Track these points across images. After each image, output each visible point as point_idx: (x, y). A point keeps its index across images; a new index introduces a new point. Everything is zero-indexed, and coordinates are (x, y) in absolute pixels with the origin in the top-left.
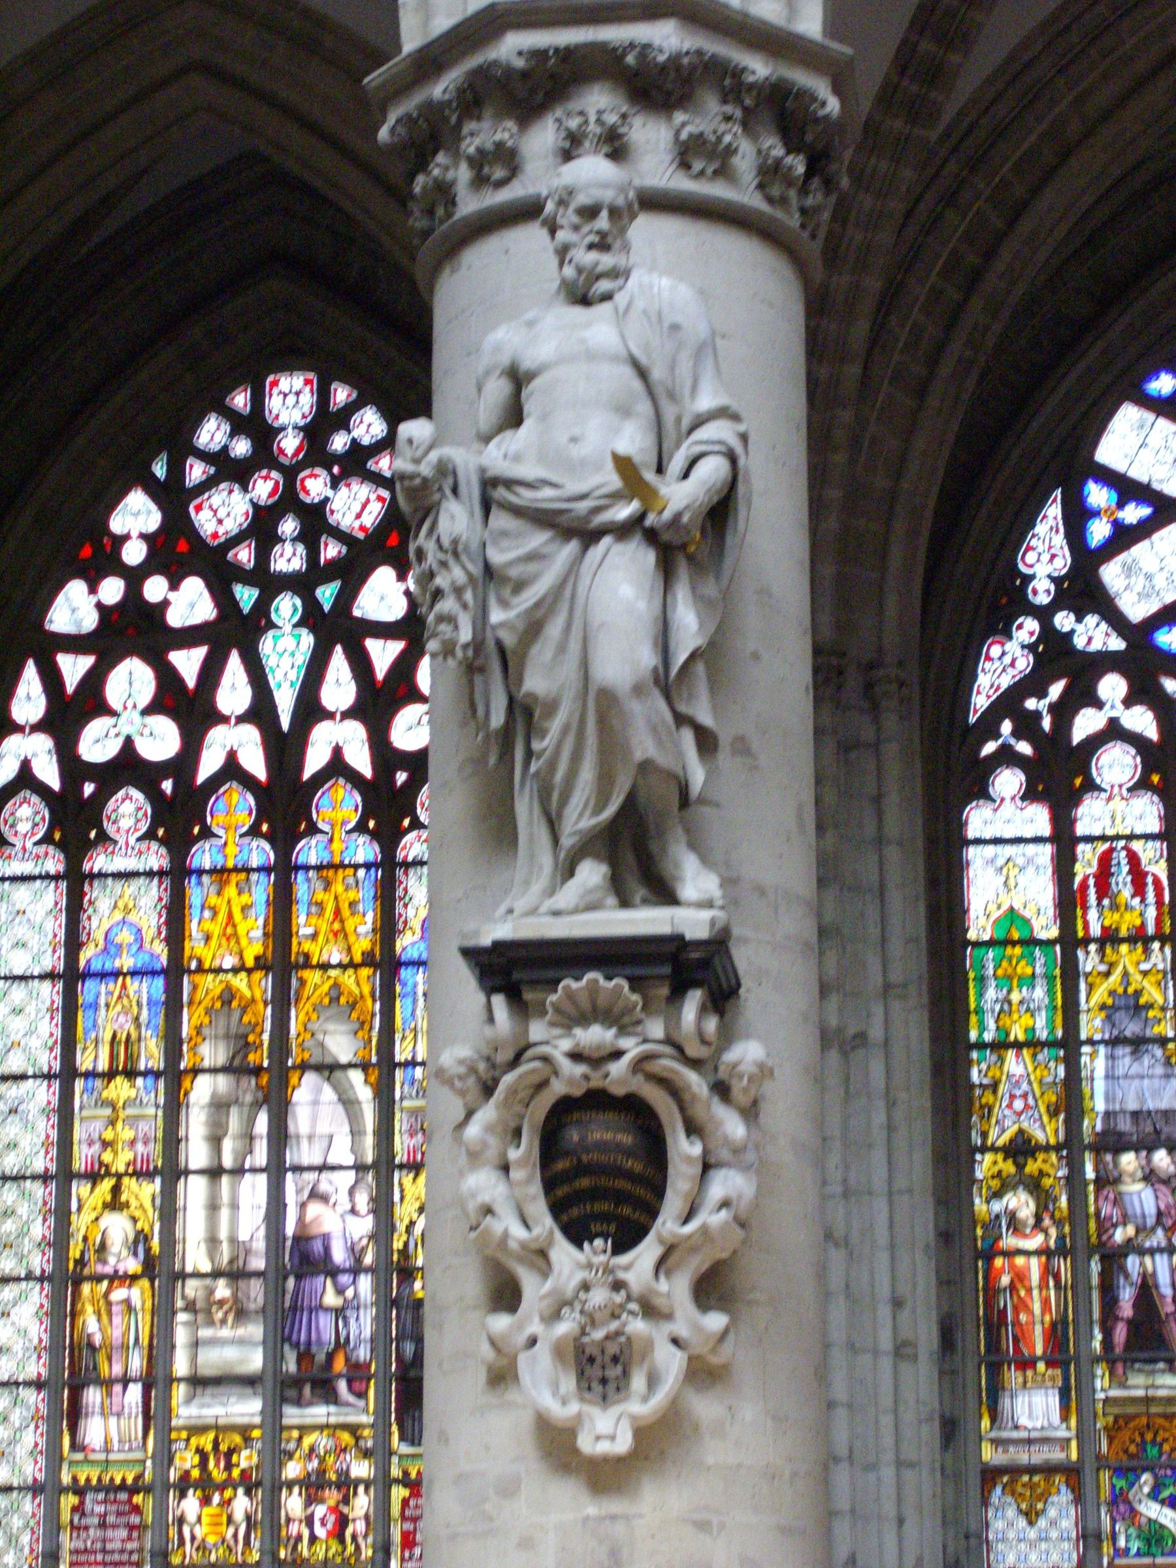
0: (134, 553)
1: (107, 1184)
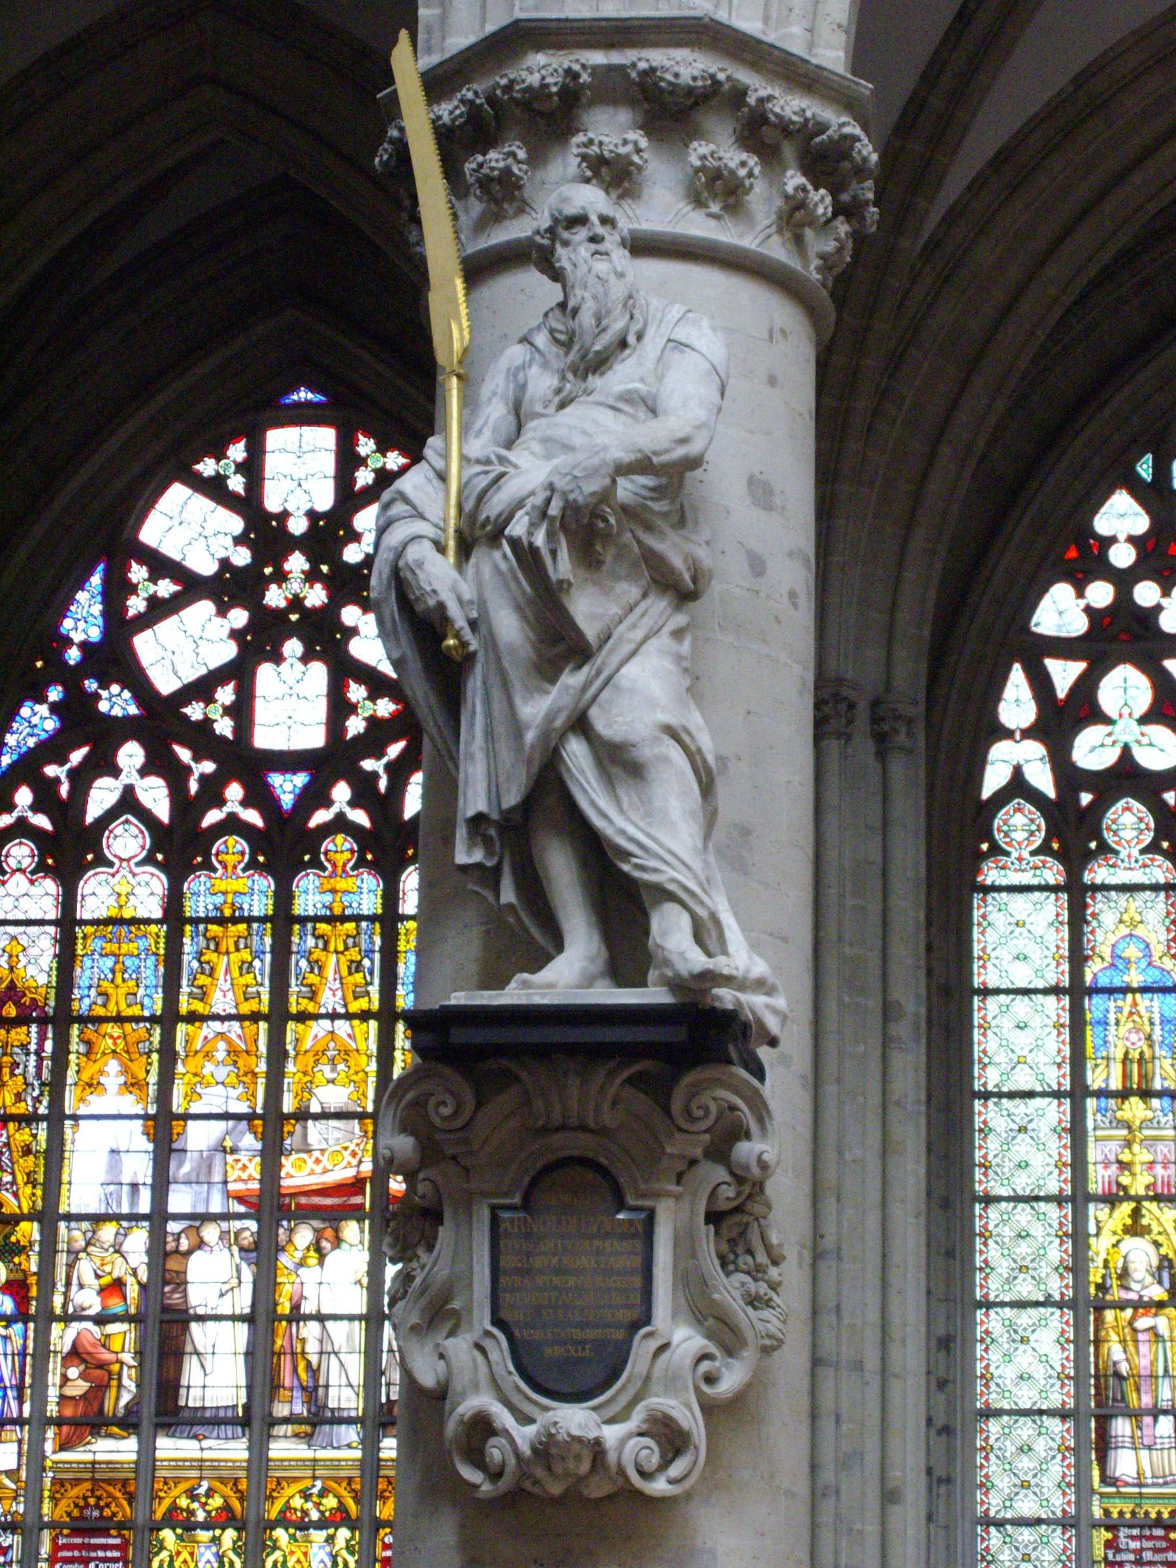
0: (1122, 556)
1: (1127, 1208)
